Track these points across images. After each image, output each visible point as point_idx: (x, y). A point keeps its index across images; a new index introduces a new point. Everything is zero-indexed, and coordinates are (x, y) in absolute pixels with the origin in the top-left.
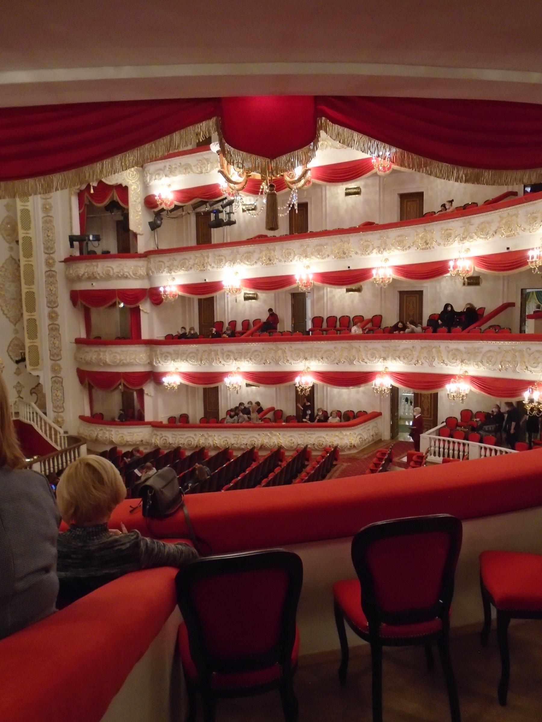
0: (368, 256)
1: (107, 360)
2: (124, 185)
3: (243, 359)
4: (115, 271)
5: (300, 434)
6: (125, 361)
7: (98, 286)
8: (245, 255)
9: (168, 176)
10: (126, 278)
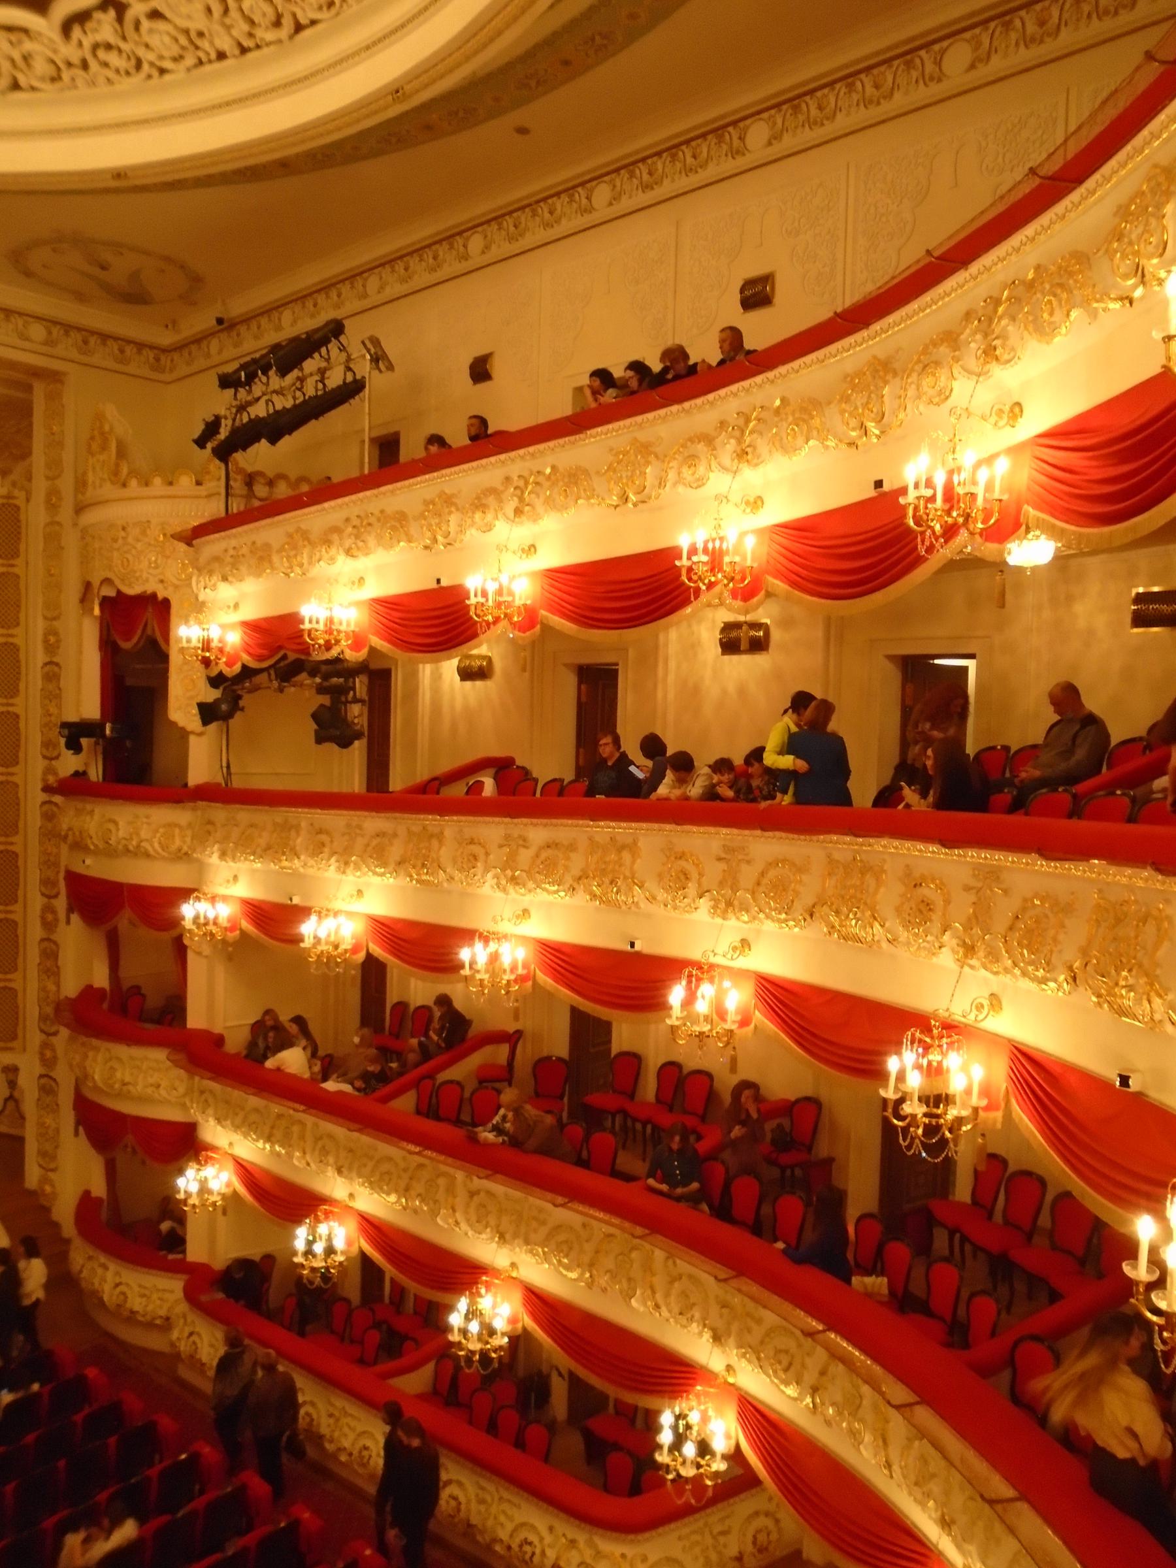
0: (687, 916)
1: (96, 1077)
2: (160, 596)
3: (354, 1174)
4: (121, 834)
5: (483, 1489)
6: (131, 1088)
7: (93, 867)
8: (374, 842)
9: (231, 583)
10: (147, 855)
